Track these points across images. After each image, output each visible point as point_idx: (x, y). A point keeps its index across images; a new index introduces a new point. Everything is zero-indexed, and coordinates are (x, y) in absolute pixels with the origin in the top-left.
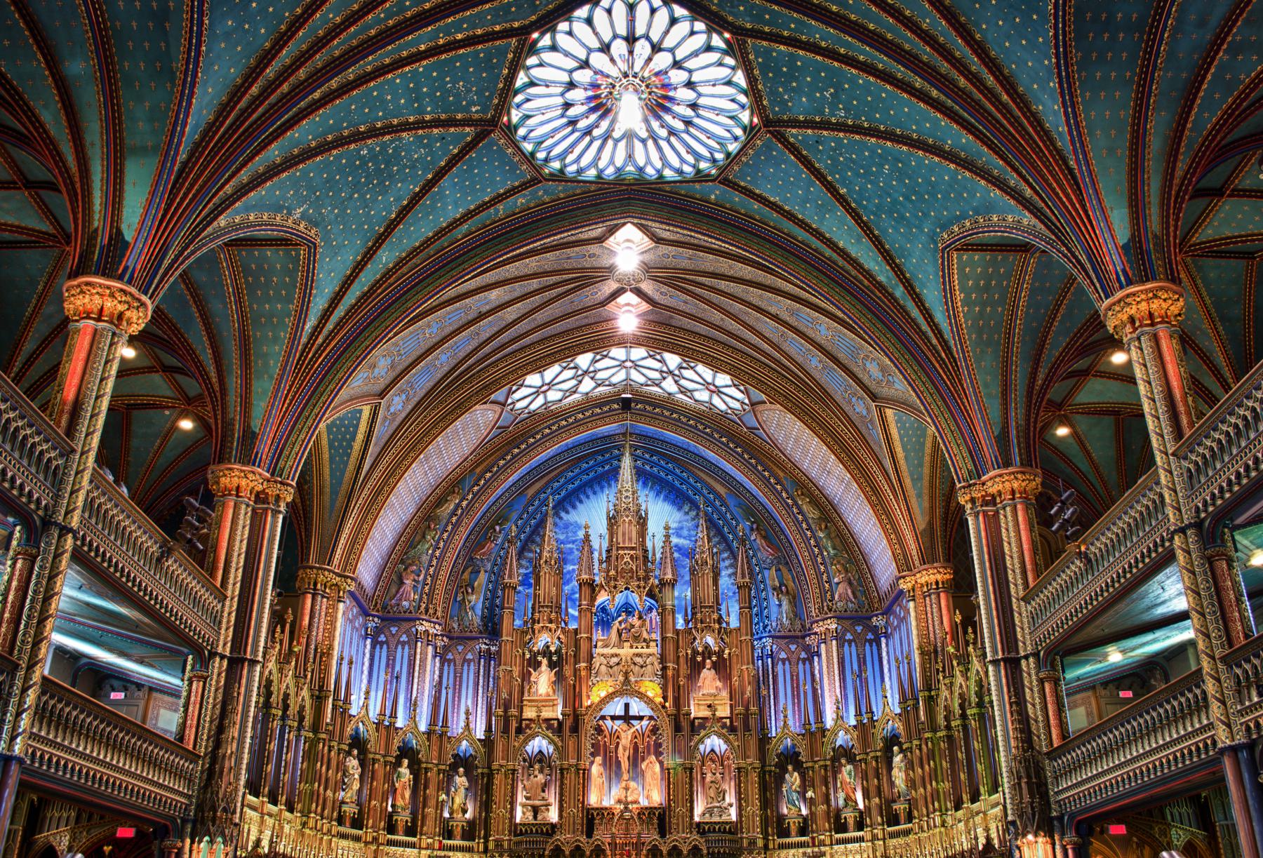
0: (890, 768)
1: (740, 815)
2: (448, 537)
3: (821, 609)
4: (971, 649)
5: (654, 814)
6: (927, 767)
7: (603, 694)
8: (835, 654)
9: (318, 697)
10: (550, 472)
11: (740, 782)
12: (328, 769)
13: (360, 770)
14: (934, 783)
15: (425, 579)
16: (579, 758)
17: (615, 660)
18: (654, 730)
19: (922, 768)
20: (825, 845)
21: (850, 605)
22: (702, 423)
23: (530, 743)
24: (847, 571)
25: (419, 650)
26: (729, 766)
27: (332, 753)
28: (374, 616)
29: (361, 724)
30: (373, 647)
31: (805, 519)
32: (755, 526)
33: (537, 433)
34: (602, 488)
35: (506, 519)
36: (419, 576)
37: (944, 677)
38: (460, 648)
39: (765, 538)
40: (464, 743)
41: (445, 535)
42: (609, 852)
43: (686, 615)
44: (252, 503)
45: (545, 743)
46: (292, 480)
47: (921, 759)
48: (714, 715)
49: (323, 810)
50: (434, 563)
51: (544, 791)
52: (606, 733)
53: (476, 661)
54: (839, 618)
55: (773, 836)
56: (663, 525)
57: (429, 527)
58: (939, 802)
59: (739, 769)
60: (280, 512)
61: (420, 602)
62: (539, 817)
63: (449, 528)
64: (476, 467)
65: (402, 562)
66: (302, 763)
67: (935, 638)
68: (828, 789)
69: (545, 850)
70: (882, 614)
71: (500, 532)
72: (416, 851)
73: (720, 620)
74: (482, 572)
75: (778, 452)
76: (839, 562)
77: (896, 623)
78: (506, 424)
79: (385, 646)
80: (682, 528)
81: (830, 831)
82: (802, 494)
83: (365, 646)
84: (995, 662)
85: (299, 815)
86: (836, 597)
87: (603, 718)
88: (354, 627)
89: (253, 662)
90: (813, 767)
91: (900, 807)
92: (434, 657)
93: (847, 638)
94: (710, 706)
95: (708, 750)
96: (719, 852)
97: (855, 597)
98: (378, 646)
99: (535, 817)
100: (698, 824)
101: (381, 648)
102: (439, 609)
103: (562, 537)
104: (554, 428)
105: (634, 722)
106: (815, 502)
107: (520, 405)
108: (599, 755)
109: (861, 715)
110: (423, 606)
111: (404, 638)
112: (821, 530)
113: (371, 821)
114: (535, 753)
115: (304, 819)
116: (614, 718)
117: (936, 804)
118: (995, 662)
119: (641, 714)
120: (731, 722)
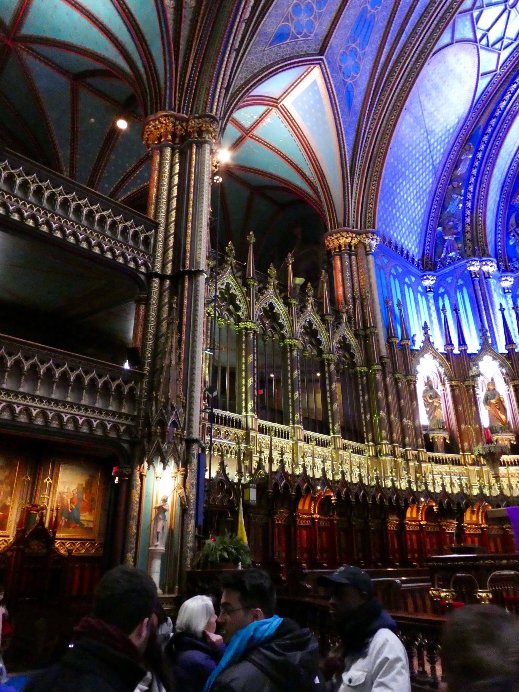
15: (463, 227)
27: (400, 384)
36: (457, 228)
41: (471, 188)
49: (404, 438)
50: (468, 212)
63: (473, 180)
66: (363, 396)
78: (493, 68)
79: (446, 296)
85: (371, 444)
88: (402, 284)
98: (440, 298)
107: (493, 36)
110: (469, 251)
111: (460, 282)
113: (466, 445)
115: (379, 447)
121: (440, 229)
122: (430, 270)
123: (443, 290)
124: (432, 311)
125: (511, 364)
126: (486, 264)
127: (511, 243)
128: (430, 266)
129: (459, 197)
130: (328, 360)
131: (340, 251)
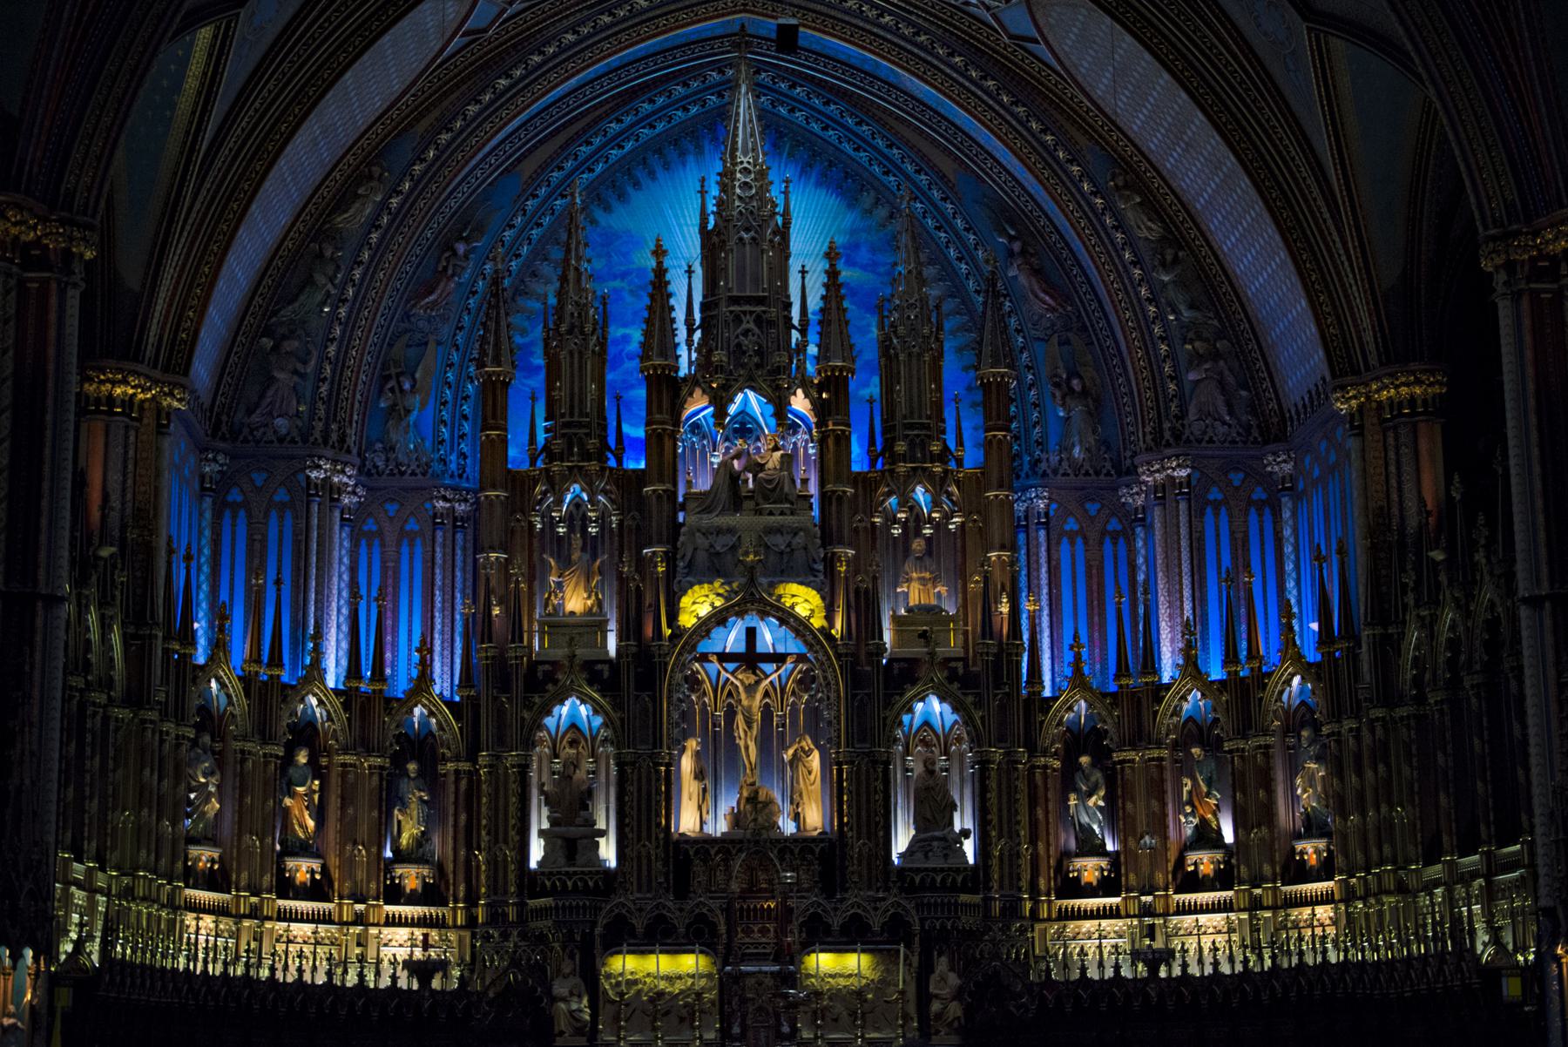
0: (1293, 769)
1: (983, 850)
2: (364, 275)
3: (1158, 433)
4: (1480, 557)
5: (812, 852)
6: (1369, 774)
7: (704, 610)
8: (1184, 531)
9: (135, 636)
10: (571, 122)
12: (160, 780)
13: (218, 776)
14: (1384, 809)
15: (320, 369)
16: (657, 743)
17: (730, 540)
18: (805, 682)
19: (1360, 773)
20: (1153, 915)
21: (1222, 429)
22: (910, 24)
23: (556, 710)
24: (1216, 356)
25: (315, 521)
26: (962, 755)
28: (217, 451)
29: (213, 681)
30: (218, 516)
31: (1130, 243)
32: (1017, 246)
33: (548, 43)
34: (683, 154)
35: (480, 229)
36: (305, 363)
37: (1417, 606)
38: (392, 508)
39: (1037, 272)
40: (417, 711)
41: (357, 274)
42: (722, 929)
43: (872, 442)
44: (15, 269)
45: (583, 710)
46: (93, 216)
47: (1358, 757)
48: (932, 654)
49: (157, 859)
50: (338, 331)
51: (586, 807)
52: (707, 686)
53: (428, 534)
55: (1048, 895)
56: (825, 248)
57: (320, 255)
58: (1393, 845)
59: (983, 763)
60: (75, 285)
61: (312, 419)
62: (580, 859)
64: (417, 120)
65: (268, 332)
67: (1402, 518)
68: (1164, 805)
69: (594, 924)
70: (1287, 452)
71: (466, 257)
72: (333, 928)
73: (945, 452)
74: (431, 346)
75: (1077, 92)
76: (1200, 338)
77: (1316, 473)
78: (483, 25)
79: (242, 513)
80: (855, 246)
82: (1126, 186)
83: (201, 514)
84: (1534, 602)
86: (1192, 410)
87: (704, 658)
89: (55, 600)
90: (1133, 761)
91: (1311, 850)
92: (342, 526)
93: (1211, 497)
94: (923, 635)
95: (917, 722)
96: (943, 926)
97: (1231, 413)
100: (901, 871)
101: (234, 517)
102: (351, 432)
103: (598, 264)
104: (585, 30)
105: (768, 667)
106: (1152, 208)
108: (693, 735)
109: (1236, 661)
111: (281, 495)
112: (1163, 264)
113: (244, 875)
114: (562, 729)
115: (126, 880)
116: (724, 657)
117: (1387, 849)
118: (1534, 602)
119: (781, 649)
120: (966, 666)
121: (267, 343)
122: (223, 439)
123: (239, 499)
124: (204, 542)
125: (349, 719)
126: (343, 472)
127: (382, 405)
128: (224, 428)
129: (329, 286)
130: (94, 704)
131: (111, 413)
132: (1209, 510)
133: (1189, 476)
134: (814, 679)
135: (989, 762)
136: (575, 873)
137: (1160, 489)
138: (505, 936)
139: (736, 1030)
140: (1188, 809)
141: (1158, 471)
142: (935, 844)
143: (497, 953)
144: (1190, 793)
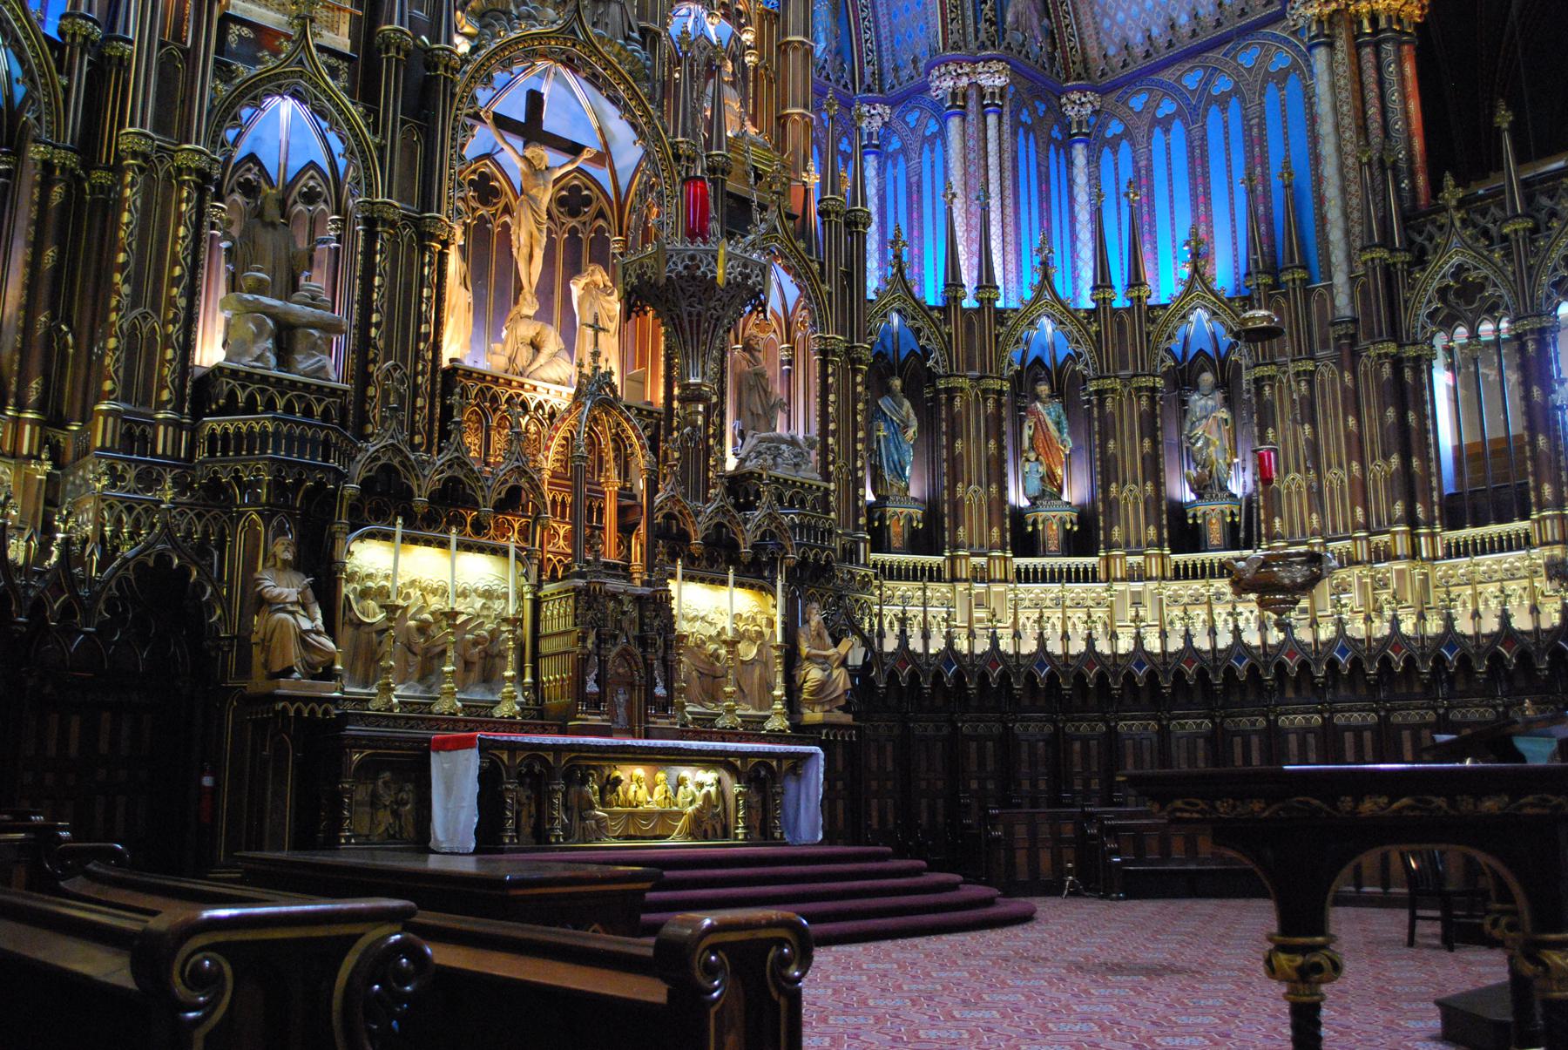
11: (825, 390)
54: (1016, 70)
62: (304, 363)
68: (1001, 447)
69: (341, 477)
81: (1004, 550)
86: (1009, 18)
99: (284, 360)
116: (502, 122)
132: (1021, 131)
133: (1002, 88)
134: (588, 201)
135: (834, 353)
136: (293, 384)
137: (960, 96)
138: (148, 480)
139: (592, 687)
140: (1032, 456)
141: (967, 74)
142: (784, 447)
143: (130, 509)
144: (1031, 439)
